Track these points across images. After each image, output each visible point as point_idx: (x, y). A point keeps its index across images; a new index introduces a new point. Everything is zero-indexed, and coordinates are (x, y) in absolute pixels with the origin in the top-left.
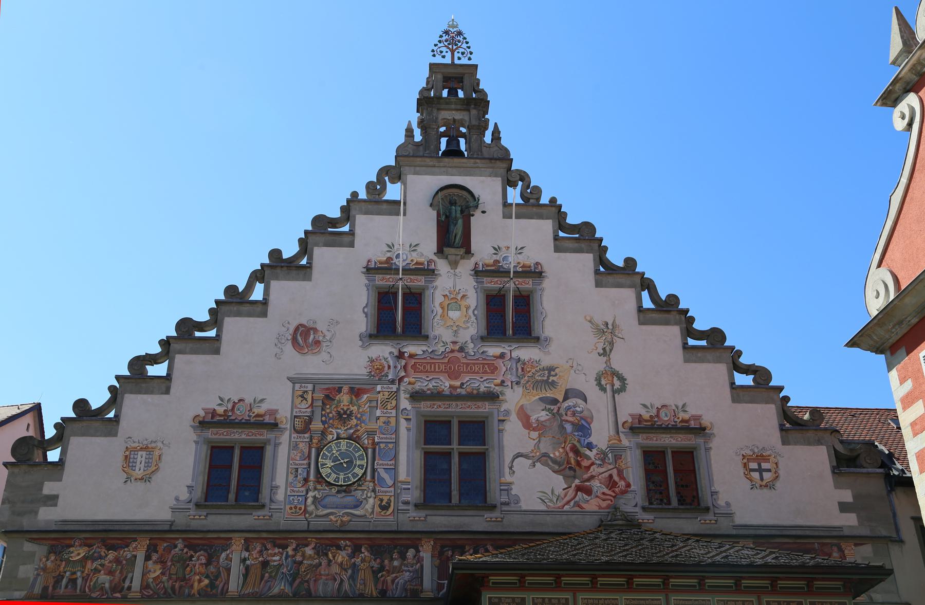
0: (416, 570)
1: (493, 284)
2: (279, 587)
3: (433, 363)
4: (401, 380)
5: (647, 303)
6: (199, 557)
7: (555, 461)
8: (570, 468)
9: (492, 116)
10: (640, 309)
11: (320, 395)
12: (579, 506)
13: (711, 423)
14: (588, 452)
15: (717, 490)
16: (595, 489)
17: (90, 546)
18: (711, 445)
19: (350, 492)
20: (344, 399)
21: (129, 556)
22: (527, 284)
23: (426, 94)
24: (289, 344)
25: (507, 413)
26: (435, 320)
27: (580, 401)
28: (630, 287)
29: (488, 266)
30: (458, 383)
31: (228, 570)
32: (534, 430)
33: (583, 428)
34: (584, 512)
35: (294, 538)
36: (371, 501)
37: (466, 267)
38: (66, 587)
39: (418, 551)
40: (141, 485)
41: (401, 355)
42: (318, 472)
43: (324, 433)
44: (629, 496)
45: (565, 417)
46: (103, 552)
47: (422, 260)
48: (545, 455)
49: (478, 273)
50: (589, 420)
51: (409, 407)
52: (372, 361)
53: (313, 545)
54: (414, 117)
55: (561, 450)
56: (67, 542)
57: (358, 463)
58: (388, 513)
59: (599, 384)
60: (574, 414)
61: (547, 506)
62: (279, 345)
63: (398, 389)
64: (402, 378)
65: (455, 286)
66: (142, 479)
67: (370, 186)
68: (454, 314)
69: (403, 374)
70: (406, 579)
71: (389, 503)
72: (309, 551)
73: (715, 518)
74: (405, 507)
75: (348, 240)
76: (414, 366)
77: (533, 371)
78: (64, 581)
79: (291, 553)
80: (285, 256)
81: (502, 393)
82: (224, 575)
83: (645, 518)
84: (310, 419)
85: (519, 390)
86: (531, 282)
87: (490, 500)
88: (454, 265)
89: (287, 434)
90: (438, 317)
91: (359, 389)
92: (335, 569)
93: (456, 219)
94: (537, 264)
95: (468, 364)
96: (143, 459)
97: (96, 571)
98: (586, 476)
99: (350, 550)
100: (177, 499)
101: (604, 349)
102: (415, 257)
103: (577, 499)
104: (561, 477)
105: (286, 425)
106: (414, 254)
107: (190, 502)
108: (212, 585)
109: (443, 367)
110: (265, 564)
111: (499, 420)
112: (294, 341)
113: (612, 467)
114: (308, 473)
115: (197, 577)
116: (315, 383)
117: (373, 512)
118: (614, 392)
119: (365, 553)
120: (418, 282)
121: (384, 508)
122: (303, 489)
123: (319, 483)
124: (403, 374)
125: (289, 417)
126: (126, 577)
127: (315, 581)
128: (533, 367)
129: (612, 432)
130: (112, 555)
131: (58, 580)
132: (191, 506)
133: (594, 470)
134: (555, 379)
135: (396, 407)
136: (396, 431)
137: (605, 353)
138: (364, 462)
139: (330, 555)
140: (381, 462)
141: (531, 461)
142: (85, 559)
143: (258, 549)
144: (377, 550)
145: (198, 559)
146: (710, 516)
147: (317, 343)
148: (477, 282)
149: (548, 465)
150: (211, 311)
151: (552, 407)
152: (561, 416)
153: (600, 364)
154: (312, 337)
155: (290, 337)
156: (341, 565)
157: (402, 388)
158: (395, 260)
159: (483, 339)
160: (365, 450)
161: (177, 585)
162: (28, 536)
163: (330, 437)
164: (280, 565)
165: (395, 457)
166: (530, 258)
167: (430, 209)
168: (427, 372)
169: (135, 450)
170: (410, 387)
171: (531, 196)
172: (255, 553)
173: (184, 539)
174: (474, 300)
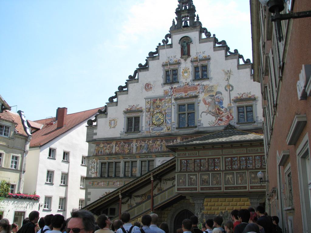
1: (195, 64)
4: (172, 95)
7: (213, 113)
9: (196, 13)
11: (152, 102)
12: (219, 124)
13: (258, 97)
14: (222, 109)
15: (258, 116)
17: (104, 144)
18: (257, 103)
19: (160, 126)
20: (158, 102)
22: (204, 63)
23: (177, 10)
25: (200, 101)
27: (220, 95)
29: (195, 59)
30: (187, 94)
31: (133, 148)
32: (207, 104)
33: (221, 103)
34: (220, 126)
36: (165, 128)
37: (189, 60)
39: (177, 140)
43: (153, 112)
44: (233, 120)
45: (216, 100)
46: (107, 145)
47: (177, 60)
48: (210, 111)
49: (191, 61)
51: (174, 102)
52: (165, 91)
53: (151, 140)
55: (214, 109)
56: (99, 143)
57: (162, 118)
64: (173, 94)
65: (186, 66)
67: (163, 41)
68: (186, 74)
69: (173, 93)
72: (151, 142)
73: (257, 124)
74: (174, 129)
75: (158, 58)
76: (175, 91)
77: (207, 88)
78: (100, 152)
81: (199, 95)
82: (132, 149)
83: (236, 126)
84: (150, 108)
85: (203, 94)
86: (207, 62)
88: (185, 60)
91: (162, 99)
92: (157, 146)
93: (185, 47)
94: (209, 56)
97: (106, 149)
98: (221, 116)
99: (160, 141)
100: (121, 132)
101: (227, 79)
102: (175, 59)
104: (214, 117)
105: (144, 111)
106: (175, 59)
108: (130, 151)
110: (141, 146)
112: (145, 87)
114: (150, 122)
116: (151, 98)
117: (166, 131)
118: (230, 91)
119: (164, 141)
121: (169, 130)
123: (153, 125)
124: (173, 93)
127: (152, 149)
129: (229, 103)
130: (108, 146)
131: (99, 152)
132: (124, 133)
133: (224, 114)
134: (213, 89)
135: (171, 103)
136: (171, 109)
137: (228, 80)
142: (103, 147)
144: (167, 141)
146: (256, 124)
147: (151, 88)
149: (211, 114)
150: (126, 83)
152: (215, 100)
153: (226, 83)
154: (149, 86)
155: (144, 87)
156: (158, 145)
157: (172, 97)
158: (170, 61)
159: (193, 80)
160: (164, 115)
163: (155, 113)
164: (144, 146)
166: (206, 55)
170: (174, 97)
171: (208, 34)
173: (123, 141)
174: (191, 69)
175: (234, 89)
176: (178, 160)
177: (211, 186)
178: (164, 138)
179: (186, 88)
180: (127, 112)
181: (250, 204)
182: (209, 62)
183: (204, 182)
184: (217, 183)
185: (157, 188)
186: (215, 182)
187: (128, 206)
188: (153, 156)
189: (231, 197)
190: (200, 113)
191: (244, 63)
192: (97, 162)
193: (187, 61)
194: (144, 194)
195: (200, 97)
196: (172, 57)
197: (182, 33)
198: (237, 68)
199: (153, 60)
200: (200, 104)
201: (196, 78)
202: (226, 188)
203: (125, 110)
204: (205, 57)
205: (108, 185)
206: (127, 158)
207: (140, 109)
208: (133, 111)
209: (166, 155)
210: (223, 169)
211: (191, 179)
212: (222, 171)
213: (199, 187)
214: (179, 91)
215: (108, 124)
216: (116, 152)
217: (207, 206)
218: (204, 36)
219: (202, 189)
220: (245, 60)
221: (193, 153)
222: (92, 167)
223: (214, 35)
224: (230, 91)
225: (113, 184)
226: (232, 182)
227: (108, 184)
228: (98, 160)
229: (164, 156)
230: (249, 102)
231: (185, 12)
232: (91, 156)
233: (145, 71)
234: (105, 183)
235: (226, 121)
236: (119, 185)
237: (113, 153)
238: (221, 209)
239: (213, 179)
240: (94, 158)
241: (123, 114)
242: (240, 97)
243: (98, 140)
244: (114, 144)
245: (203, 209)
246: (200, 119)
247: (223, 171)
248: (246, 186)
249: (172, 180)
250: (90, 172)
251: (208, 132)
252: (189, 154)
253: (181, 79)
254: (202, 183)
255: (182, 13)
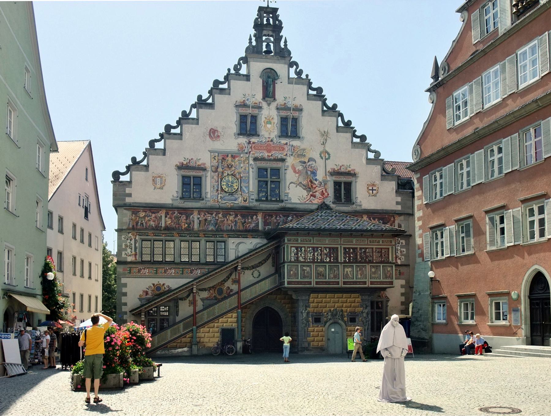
0: (257, 223)
1: (284, 114)
2: (211, 228)
3: (262, 146)
4: (250, 152)
5: (341, 124)
6: (183, 217)
7: (304, 185)
8: (309, 188)
10: (338, 127)
11: (220, 158)
14: (315, 182)
16: (317, 196)
17: (146, 212)
20: (229, 159)
21: (159, 216)
22: (296, 114)
24: (208, 136)
25: (288, 166)
26: (262, 128)
27: (314, 163)
28: (334, 116)
29: (282, 105)
30: (270, 155)
31: (194, 222)
32: (297, 173)
33: (314, 173)
34: (313, 204)
35: (215, 211)
36: (240, 198)
37: (274, 105)
38: (140, 226)
39: (257, 217)
40: (160, 190)
41: (249, 143)
42: (221, 187)
43: (223, 173)
45: (308, 169)
46: (150, 214)
47: (256, 102)
48: (301, 183)
49: (277, 109)
50: (316, 170)
51: (253, 163)
52: (239, 145)
53: (221, 214)
54: (253, 32)
55: (306, 181)
56: (138, 210)
58: (246, 203)
59: (321, 156)
60: (311, 167)
61: (301, 201)
62: (204, 137)
63: (249, 156)
66: (160, 188)
68: (269, 126)
69: (250, 150)
70: (253, 226)
71: (247, 199)
72: (220, 215)
74: (252, 201)
79: (214, 216)
80: (203, 98)
82: (192, 223)
83: (332, 206)
84: (218, 167)
85: (292, 157)
87: (281, 199)
88: (269, 105)
89: (210, 172)
90: (263, 127)
91: (235, 156)
93: (270, 85)
95: (274, 147)
96: (159, 181)
97: (149, 220)
98: (314, 191)
99: (234, 216)
100: (173, 196)
101: (323, 142)
103: (311, 199)
105: (209, 169)
106: (254, 99)
107: (177, 197)
108: (189, 226)
109: (265, 148)
110: (206, 220)
111: (285, 169)
112: (210, 134)
113: (323, 188)
114: (218, 187)
115: (183, 224)
117: (241, 202)
119: (239, 217)
120: (256, 111)
121: (245, 201)
122: (216, 193)
123: (222, 191)
125: (210, 166)
126: (159, 223)
128: (297, 149)
129: (324, 175)
130: (154, 215)
131: (137, 223)
132: (178, 198)
133: (317, 189)
134: (305, 153)
136: (248, 173)
137: (323, 144)
138: (237, 184)
139: (228, 217)
140: (243, 184)
141: (295, 185)
142: (145, 216)
143: (203, 214)
144: (243, 216)
145: (183, 217)
146: (354, 206)
147: (218, 136)
148: (278, 112)
149: (301, 187)
151: (304, 165)
152: (306, 168)
153: (321, 148)
154: (216, 134)
155: (208, 134)
156: (231, 221)
157: (250, 156)
158: (247, 102)
159: (279, 137)
160: (238, 179)
161: (177, 226)
162: (125, 208)
163: (225, 174)
165: (248, 182)
166: (297, 103)
167: (260, 79)
168: (259, 149)
169: (156, 177)
170: (253, 155)
171: (299, 73)
172: (202, 216)
174: (276, 120)
175: (331, 158)
176: (288, 246)
177: (327, 280)
178: (239, 212)
179: (269, 146)
180: (181, 167)
181: (361, 301)
182: (301, 114)
183: (319, 275)
184: (335, 277)
185: (231, 278)
186: (332, 276)
187: (189, 303)
188: (224, 236)
189: (341, 293)
190: (288, 184)
191: (343, 126)
192: (135, 239)
193: (270, 107)
194: (213, 287)
195: (287, 162)
196: (249, 95)
197: (264, 62)
198: (335, 131)
199: (220, 94)
200: (288, 172)
201: (284, 134)
202: (345, 283)
203: (178, 164)
204: (295, 106)
205: (156, 273)
206: (185, 236)
207: (202, 166)
208: (191, 167)
209: (243, 236)
210: (341, 260)
211: (304, 270)
212: (341, 263)
213: (314, 280)
214: (259, 148)
215: (151, 182)
216: (167, 226)
217: (313, 302)
218: (293, 75)
219: (317, 283)
220: (346, 121)
221: (306, 239)
222: (126, 246)
223: (307, 76)
224: (326, 159)
225: (165, 272)
226: (351, 276)
227: (157, 271)
228: (137, 236)
229: (240, 236)
230: (348, 177)
231: (268, 29)
232: (124, 230)
233: (209, 109)
234: (151, 270)
235: (320, 198)
236: (174, 273)
237: (161, 227)
238: (330, 306)
239: (330, 272)
240: (129, 233)
241: (176, 169)
242: (338, 169)
243: (134, 205)
244: (162, 213)
245: (309, 307)
246: (287, 191)
247: (341, 263)
248: (339, 282)
249: (252, 269)
250: (123, 253)
251: (298, 209)
252: (301, 241)
253: (262, 132)
254: (317, 276)
255: (265, 28)
